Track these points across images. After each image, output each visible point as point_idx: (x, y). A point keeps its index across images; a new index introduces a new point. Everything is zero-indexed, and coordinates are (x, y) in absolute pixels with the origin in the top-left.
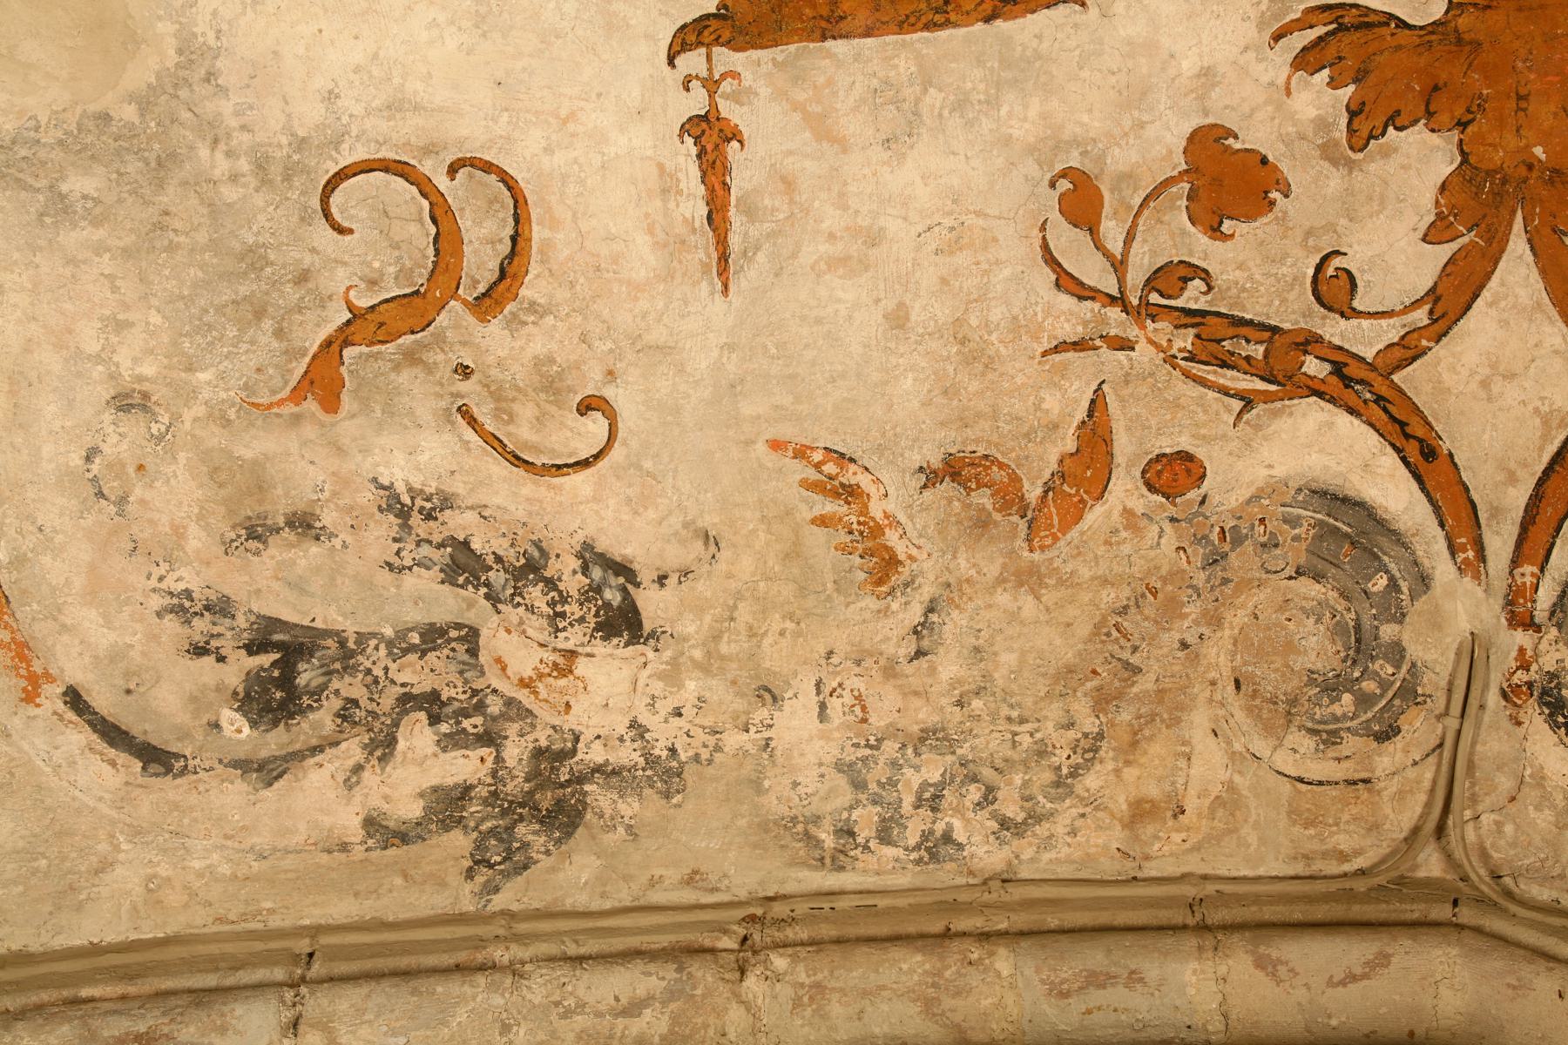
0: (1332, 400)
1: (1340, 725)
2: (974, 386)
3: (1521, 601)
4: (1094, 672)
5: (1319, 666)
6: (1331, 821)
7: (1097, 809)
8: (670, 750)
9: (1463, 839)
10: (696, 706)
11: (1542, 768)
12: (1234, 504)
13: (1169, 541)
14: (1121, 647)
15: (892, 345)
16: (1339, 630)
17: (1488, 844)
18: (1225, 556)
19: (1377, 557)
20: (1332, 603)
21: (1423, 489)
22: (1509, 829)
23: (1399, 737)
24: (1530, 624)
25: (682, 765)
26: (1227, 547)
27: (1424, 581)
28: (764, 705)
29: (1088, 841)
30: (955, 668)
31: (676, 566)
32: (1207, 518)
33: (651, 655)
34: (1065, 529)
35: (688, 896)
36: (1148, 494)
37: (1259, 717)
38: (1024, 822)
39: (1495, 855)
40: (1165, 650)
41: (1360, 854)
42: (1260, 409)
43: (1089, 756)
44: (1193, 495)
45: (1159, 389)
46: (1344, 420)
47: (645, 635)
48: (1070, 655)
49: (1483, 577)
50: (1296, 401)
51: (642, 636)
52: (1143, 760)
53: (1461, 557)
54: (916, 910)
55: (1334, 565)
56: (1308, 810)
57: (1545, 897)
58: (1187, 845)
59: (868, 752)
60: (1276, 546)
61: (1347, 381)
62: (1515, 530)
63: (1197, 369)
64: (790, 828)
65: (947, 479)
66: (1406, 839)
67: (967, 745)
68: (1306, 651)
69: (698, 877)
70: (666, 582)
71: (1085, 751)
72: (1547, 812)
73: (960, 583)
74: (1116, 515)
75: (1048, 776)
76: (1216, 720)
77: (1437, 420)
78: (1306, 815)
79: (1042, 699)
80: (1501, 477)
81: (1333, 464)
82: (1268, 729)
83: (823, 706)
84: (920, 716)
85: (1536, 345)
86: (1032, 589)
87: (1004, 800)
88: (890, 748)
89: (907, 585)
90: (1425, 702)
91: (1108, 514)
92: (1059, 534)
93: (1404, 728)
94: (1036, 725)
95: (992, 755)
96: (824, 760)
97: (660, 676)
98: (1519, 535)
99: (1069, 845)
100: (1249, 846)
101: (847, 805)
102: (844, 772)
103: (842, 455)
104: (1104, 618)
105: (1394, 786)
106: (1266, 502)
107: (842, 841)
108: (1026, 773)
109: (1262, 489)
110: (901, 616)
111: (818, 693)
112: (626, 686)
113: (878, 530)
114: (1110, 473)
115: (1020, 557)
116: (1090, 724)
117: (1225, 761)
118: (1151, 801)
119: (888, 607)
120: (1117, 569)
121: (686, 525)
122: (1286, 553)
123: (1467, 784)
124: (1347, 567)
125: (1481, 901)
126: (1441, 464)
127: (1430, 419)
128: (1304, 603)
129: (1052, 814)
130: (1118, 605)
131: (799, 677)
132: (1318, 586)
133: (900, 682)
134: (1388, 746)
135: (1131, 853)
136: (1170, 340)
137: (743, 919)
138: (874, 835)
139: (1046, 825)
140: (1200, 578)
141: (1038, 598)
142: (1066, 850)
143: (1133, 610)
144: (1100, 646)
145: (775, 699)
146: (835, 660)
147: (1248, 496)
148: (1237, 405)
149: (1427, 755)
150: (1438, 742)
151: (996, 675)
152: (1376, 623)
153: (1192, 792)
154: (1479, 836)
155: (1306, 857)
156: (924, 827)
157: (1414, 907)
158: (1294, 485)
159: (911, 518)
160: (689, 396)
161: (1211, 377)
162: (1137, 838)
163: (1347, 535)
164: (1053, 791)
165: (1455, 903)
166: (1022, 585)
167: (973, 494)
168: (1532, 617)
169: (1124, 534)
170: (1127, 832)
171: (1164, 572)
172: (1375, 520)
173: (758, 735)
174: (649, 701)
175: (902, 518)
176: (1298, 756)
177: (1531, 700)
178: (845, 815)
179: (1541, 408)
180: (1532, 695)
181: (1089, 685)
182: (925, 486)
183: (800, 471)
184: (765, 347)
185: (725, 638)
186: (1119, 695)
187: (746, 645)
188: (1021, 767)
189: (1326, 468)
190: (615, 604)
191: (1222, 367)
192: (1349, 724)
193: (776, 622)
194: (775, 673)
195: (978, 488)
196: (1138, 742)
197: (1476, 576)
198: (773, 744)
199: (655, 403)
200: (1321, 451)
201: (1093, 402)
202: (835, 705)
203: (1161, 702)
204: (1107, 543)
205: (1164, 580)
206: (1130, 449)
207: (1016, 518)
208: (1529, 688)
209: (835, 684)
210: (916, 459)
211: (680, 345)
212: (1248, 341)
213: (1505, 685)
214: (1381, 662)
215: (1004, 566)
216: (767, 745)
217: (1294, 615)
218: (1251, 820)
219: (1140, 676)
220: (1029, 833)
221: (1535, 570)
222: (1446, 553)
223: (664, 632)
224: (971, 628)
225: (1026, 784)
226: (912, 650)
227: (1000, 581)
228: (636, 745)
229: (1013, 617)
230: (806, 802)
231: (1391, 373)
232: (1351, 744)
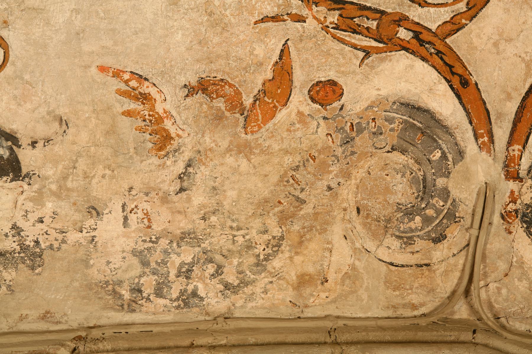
0: (413, 53)
1: (414, 234)
2: (216, 40)
3: (513, 165)
4: (280, 202)
5: (403, 201)
6: (408, 287)
7: (279, 279)
8: (35, 242)
9: (479, 296)
10: (52, 217)
11: (522, 257)
12: (358, 110)
13: (323, 130)
14: (295, 189)
15: (170, 14)
16: (414, 181)
17: (493, 300)
18: (353, 139)
19: (436, 141)
20: (411, 166)
21: (461, 103)
22: (504, 291)
23: (446, 241)
24: (517, 177)
25: (42, 250)
26: (354, 134)
27: (461, 154)
28: (91, 217)
29: (273, 297)
30: (201, 199)
31: (42, 137)
32: (343, 118)
33: (26, 187)
34: (265, 122)
35: (43, 326)
36: (312, 103)
37: (370, 229)
38: (238, 286)
39: (497, 306)
40: (319, 191)
41: (423, 305)
42: (373, 57)
43: (275, 249)
44: (337, 105)
45: (319, 45)
46: (419, 64)
47: (23, 175)
48: (266, 193)
49: (492, 152)
50: (393, 53)
51: (21, 176)
52: (305, 252)
53: (481, 140)
54: (175, 333)
55: (413, 145)
56: (396, 280)
57: (523, 329)
58: (329, 300)
59: (151, 245)
60: (381, 134)
61: (422, 42)
62: (510, 126)
63: (340, 34)
64: (105, 288)
65: (200, 92)
66: (448, 297)
67: (207, 242)
68: (396, 192)
69: (49, 315)
70: (37, 145)
71: (274, 246)
72: (524, 282)
73: (206, 151)
74: (293, 115)
75: (252, 260)
76: (346, 230)
77: (469, 64)
78: (394, 283)
79: (250, 217)
80: (503, 96)
81: (412, 89)
82: (374, 236)
83: (126, 219)
84: (181, 225)
85: (524, 23)
86: (246, 155)
87: (228, 273)
88: (164, 243)
89: (175, 151)
90: (460, 221)
91: (289, 114)
92: (262, 125)
93: (449, 235)
94: (246, 231)
95: (221, 247)
96: (125, 249)
97: (31, 199)
98: (512, 128)
99: (263, 299)
100: (363, 300)
101: (138, 275)
102: (137, 256)
103: (141, 76)
104: (286, 172)
105: (442, 268)
106: (376, 109)
107: (134, 295)
108: (240, 258)
109: (374, 102)
110: (172, 168)
111: (123, 211)
112: (11, 205)
113: (160, 120)
114: (291, 91)
115: (240, 137)
116: (276, 232)
117: (351, 253)
118: (309, 275)
119: (165, 163)
120: (293, 145)
121: (49, 113)
122: (386, 138)
123: (482, 267)
124: (419, 146)
125: (489, 331)
126: (471, 89)
127: (466, 64)
128: (396, 166)
129: (254, 281)
130: (294, 165)
131: (113, 201)
132: (403, 157)
133: (170, 206)
134: (440, 246)
135: (297, 304)
136: (325, 17)
137: (74, 339)
138: (153, 292)
139: (250, 287)
140: (339, 151)
141: (249, 160)
142: (261, 302)
143: (302, 168)
144: (282, 188)
145: (98, 214)
146: (133, 192)
147: (366, 106)
148: (361, 54)
149: (461, 251)
150: (466, 243)
151: (225, 203)
152: (434, 177)
153: (332, 270)
154: (488, 296)
155: (394, 307)
156: (181, 288)
157: (452, 334)
158: (391, 100)
159: (179, 113)
160: (52, 38)
161: (347, 39)
162: (301, 295)
163: (419, 128)
164: (255, 268)
165: (474, 332)
166: (240, 153)
167: (214, 101)
168: (518, 174)
169: (298, 126)
170: (295, 292)
171: (319, 147)
172: (435, 120)
173: (88, 234)
174: (24, 213)
175: (174, 113)
176: (391, 251)
177: (517, 220)
178: (137, 280)
179: (525, 58)
180: (517, 217)
181: (276, 209)
182: (187, 96)
183: (116, 84)
184: (97, 12)
185: (70, 179)
186: (293, 216)
187: (82, 183)
188: (237, 255)
189: (409, 91)
190: (5, 157)
191: (353, 33)
192: (419, 233)
193: (100, 170)
194: (99, 199)
195: (217, 97)
196: (302, 242)
197: (489, 151)
198: (96, 239)
199: (32, 41)
200: (406, 81)
201: (282, 51)
202: (133, 218)
203: (316, 219)
204: (288, 130)
205: (319, 152)
206: (302, 78)
207: (238, 115)
208: (516, 213)
209: (133, 206)
210: (183, 80)
211: (47, 8)
212: (368, 19)
213: (503, 212)
214: (437, 199)
215: (231, 142)
216: (93, 240)
217: (390, 173)
218: (364, 286)
219: (305, 205)
220: (241, 292)
221: (520, 147)
222: (472, 139)
223: (34, 174)
224: (211, 176)
225: (240, 264)
226: (178, 188)
227: (229, 150)
228: (15, 239)
229: (235, 170)
230: (114, 273)
231: (445, 38)
232: (420, 244)
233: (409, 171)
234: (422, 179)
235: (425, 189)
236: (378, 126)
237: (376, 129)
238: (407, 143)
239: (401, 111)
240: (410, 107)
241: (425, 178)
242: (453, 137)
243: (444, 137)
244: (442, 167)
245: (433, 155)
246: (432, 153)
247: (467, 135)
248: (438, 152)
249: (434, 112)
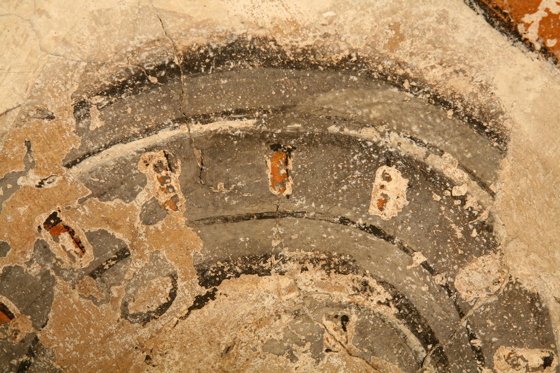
19: (351, 141)
20: (321, 295)
122: (154, 257)
124: (300, 203)
152: (439, 279)
172: (288, 64)
214: (504, 351)
233: (329, 318)
234: (399, 316)
235: (435, 342)
236: (91, 236)
237: (89, 251)
238: (245, 224)
239: (132, 122)
240: (154, 80)
241: (408, 305)
242: (406, 85)
243: (370, 105)
244: (443, 223)
245: (374, 202)
246: (367, 199)
247: (461, 38)
248: (389, 179)
249: (261, 33)
